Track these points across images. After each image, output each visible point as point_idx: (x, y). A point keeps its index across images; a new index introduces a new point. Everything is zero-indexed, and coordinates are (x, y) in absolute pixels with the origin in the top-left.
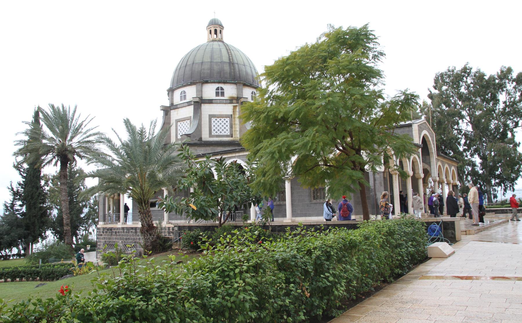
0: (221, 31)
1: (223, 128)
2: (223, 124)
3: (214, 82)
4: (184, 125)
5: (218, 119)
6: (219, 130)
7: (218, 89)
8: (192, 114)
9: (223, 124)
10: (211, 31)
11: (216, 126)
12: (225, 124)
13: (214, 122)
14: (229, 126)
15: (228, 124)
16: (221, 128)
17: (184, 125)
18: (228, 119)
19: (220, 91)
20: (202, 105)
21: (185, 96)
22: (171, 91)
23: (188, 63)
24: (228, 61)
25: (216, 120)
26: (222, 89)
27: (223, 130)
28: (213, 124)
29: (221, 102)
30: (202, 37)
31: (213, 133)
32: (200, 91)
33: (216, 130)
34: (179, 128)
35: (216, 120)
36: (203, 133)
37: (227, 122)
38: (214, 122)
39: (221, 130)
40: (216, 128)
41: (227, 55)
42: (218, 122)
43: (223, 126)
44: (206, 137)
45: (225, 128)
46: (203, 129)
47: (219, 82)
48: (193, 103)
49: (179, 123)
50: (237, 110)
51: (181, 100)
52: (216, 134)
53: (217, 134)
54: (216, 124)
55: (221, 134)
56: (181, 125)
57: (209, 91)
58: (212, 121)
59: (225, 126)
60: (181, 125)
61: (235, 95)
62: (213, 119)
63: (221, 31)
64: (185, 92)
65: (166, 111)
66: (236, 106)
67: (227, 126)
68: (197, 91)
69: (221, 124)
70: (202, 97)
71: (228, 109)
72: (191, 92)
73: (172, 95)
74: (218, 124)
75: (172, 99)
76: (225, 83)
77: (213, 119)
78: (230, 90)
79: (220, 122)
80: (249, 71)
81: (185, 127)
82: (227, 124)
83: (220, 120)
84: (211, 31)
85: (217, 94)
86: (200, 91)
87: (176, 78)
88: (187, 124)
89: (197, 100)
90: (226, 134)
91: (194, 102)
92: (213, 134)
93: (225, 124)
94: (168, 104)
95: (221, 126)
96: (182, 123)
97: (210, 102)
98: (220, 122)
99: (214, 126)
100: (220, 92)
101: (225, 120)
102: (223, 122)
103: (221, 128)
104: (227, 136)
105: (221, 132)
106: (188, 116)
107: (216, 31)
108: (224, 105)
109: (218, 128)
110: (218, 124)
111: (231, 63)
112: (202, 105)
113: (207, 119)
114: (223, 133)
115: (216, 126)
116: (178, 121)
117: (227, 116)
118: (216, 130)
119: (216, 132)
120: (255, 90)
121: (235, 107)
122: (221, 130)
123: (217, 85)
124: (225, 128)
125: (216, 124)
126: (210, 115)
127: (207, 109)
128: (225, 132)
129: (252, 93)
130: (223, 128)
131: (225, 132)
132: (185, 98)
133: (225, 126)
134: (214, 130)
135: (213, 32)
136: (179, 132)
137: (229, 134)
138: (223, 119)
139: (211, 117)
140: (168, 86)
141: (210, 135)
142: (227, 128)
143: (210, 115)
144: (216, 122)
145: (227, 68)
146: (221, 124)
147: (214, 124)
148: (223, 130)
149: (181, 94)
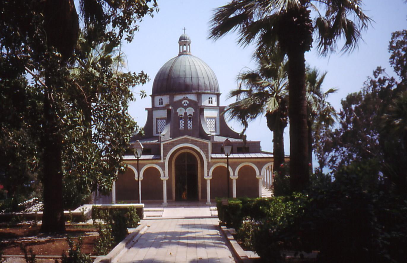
4: (162, 123)
21: (162, 102)
30: (175, 50)
34: (158, 124)
49: (159, 121)
51: (160, 104)
64: (162, 100)
72: (166, 99)
94: (150, 106)
116: (157, 119)
140: (151, 94)
149: (160, 100)
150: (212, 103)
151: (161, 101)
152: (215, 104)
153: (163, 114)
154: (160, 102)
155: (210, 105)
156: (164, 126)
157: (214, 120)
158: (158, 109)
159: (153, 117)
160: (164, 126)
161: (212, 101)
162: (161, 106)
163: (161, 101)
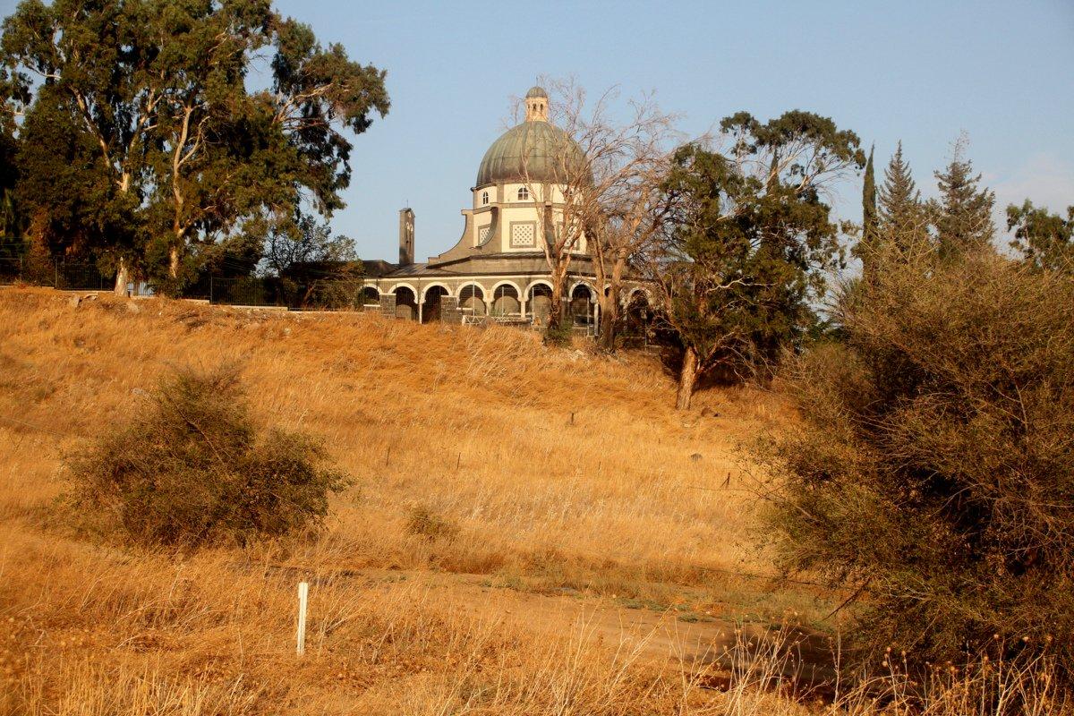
7: (521, 190)
18: (531, 226)
26: (525, 190)
32: (500, 196)
39: (523, 240)
57: (511, 190)
77: (515, 226)
85: (520, 196)
86: (500, 196)
97: (512, 205)
100: (522, 194)
114: (526, 243)
117: (530, 222)
122: (523, 240)
139: (512, 224)
141: (511, 246)
153: (487, 218)
162: (487, 205)
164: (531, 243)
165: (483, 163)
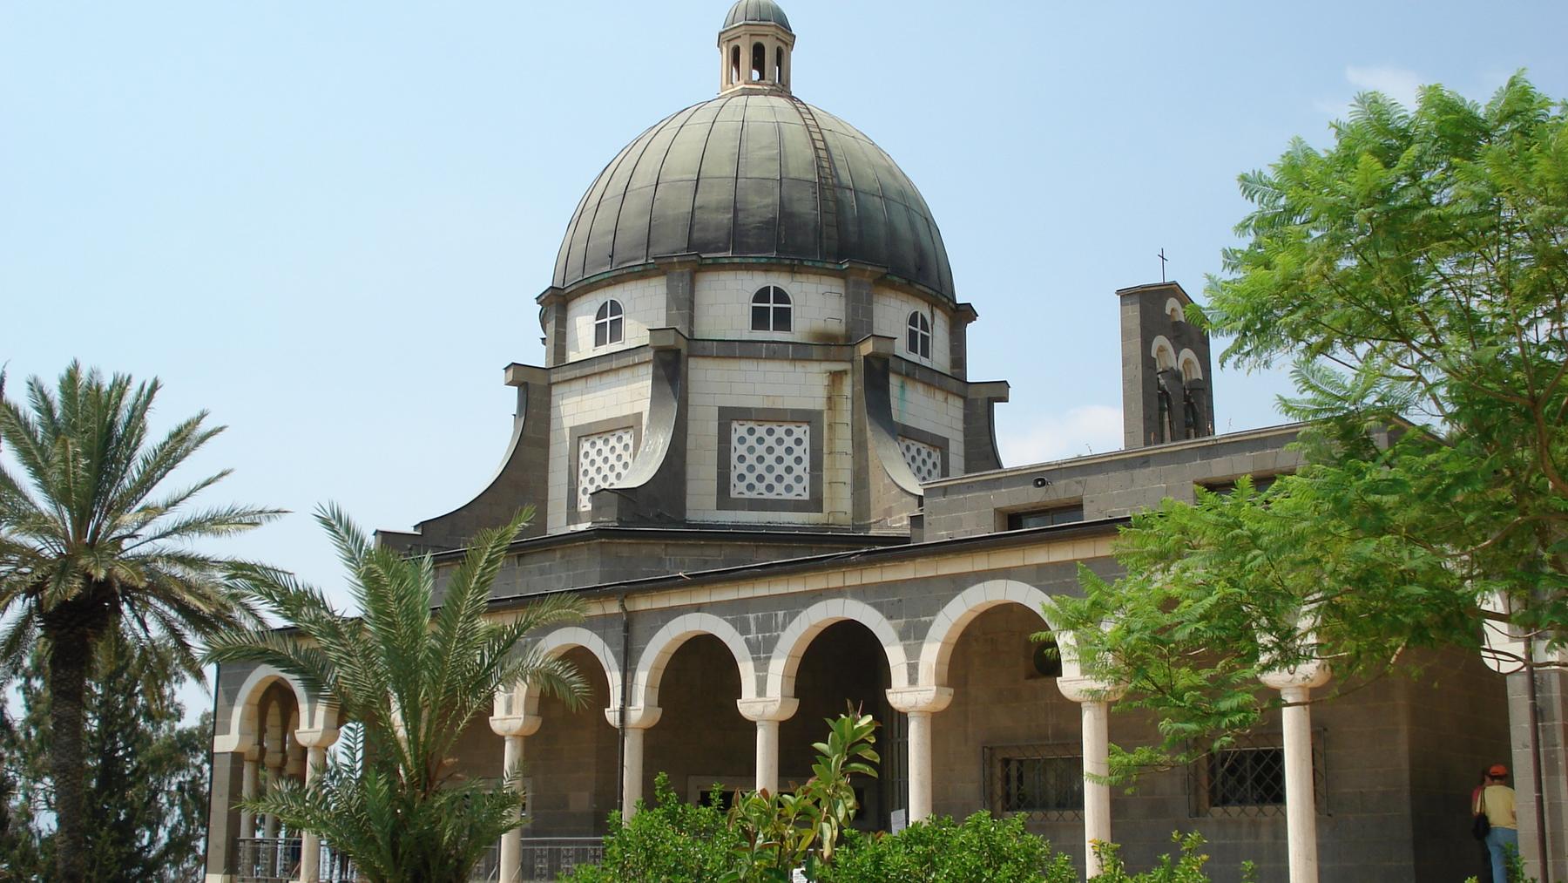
0: (779, 53)
1: (780, 469)
2: (780, 451)
3: (748, 267)
5: (761, 431)
6: (760, 478)
7: (762, 295)
8: (644, 406)
9: (780, 451)
10: (736, 52)
11: (751, 459)
12: (789, 450)
13: (742, 440)
14: (806, 462)
15: (803, 452)
16: (770, 469)
17: (606, 451)
18: (802, 431)
19: (771, 305)
20: (692, 362)
21: (617, 324)
22: (556, 304)
23: (635, 184)
24: (812, 176)
25: (751, 431)
26: (781, 296)
27: (779, 478)
28: (738, 450)
29: (775, 352)
31: (738, 490)
32: (684, 304)
33: (751, 478)
35: (751, 431)
36: (691, 487)
37: (799, 442)
38: (742, 440)
39: (770, 478)
40: (751, 468)
41: (810, 153)
42: (760, 440)
43: (780, 460)
44: (702, 506)
45: (789, 470)
46: (691, 472)
47: (767, 268)
48: (649, 355)
49: (586, 446)
50: (847, 388)
52: (748, 495)
53: (753, 495)
54: (751, 450)
55: (772, 496)
56: (593, 454)
57: (727, 302)
58: (734, 438)
59: (789, 460)
60: (593, 454)
61: (837, 327)
62: (739, 430)
63: (779, 53)
64: (616, 308)
65: (534, 391)
66: (845, 372)
67: (798, 460)
68: (673, 301)
69: (770, 450)
70: (691, 333)
71: (804, 386)
73: (562, 323)
74: (761, 450)
75: (559, 344)
76: (793, 270)
77: (739, 430)
78: (816, 303)
79: (770, 441)
80: (902, 226)
81: (612, 459)
82: (798, 451)
83: (770, 432)
84: (736, 52)
85: (759, 319)
86: (684, 304)
87: (579, 249)
88: (619, 448)
89: (669, 341)
90: (791, 496)
91: (659, 351)
92: (734, 494)
93: (789, 450)
94: (538, 356)
95: (770, 460)
96: (600, 444)
98: (770, 441)
99: (742, 458)
100: (771, 310)
101: (789, 432)
102: (780, 441)
103: (770, 469)
104: (797, 506)
105: (770, 488)
106: (627, 410)
107: (758, 51)
108: (787, 366)
109: (760, 469)
110: (761, 450)
111: (824, 157)
112: (692, 362)
113: (713, 427)
114: (780, 492)
115: (751, 459)
118: (751, 478)
119: (751, 487)
120: (924, 310)
121: (836, 376)
122: (770, 478)
123: (758, 281)
124: (789, 470)
125: (751, 450)
126: (720, 409)
127: (715, 384)
128: (789, 488)
129: (913, 320)
130: (780, 469)
131: (789, 488)
132: (616, 335)
133: (789, 460)
134: (741, 477)
135: (746, 57)
136: (584, 482)
137: (806, 496)
138: (780, 431)
139: (728, 416)
141: (724, 499)
142: (798, 470)
143: (720, 409)
144: (751, 440)
145: (806, 206)
146: (770, 450)
147: (742, 450)
148: (779, 478)
149: (601, 313)
150: (925, 353)
151: (608, 319)
152: (939, 358)
154: (600, 328)
155: (915, 358)
156: (619, 468)
157: (936, 456)
158: (592, 370)
159: (554, 425)
160: (619, 468)
161: (925, 339)
163: (608, 319)
164: (802, 492)
165: (575, 222)
